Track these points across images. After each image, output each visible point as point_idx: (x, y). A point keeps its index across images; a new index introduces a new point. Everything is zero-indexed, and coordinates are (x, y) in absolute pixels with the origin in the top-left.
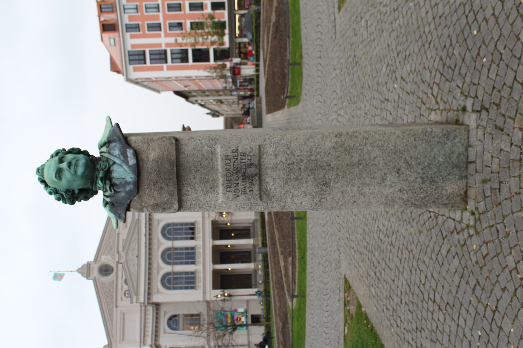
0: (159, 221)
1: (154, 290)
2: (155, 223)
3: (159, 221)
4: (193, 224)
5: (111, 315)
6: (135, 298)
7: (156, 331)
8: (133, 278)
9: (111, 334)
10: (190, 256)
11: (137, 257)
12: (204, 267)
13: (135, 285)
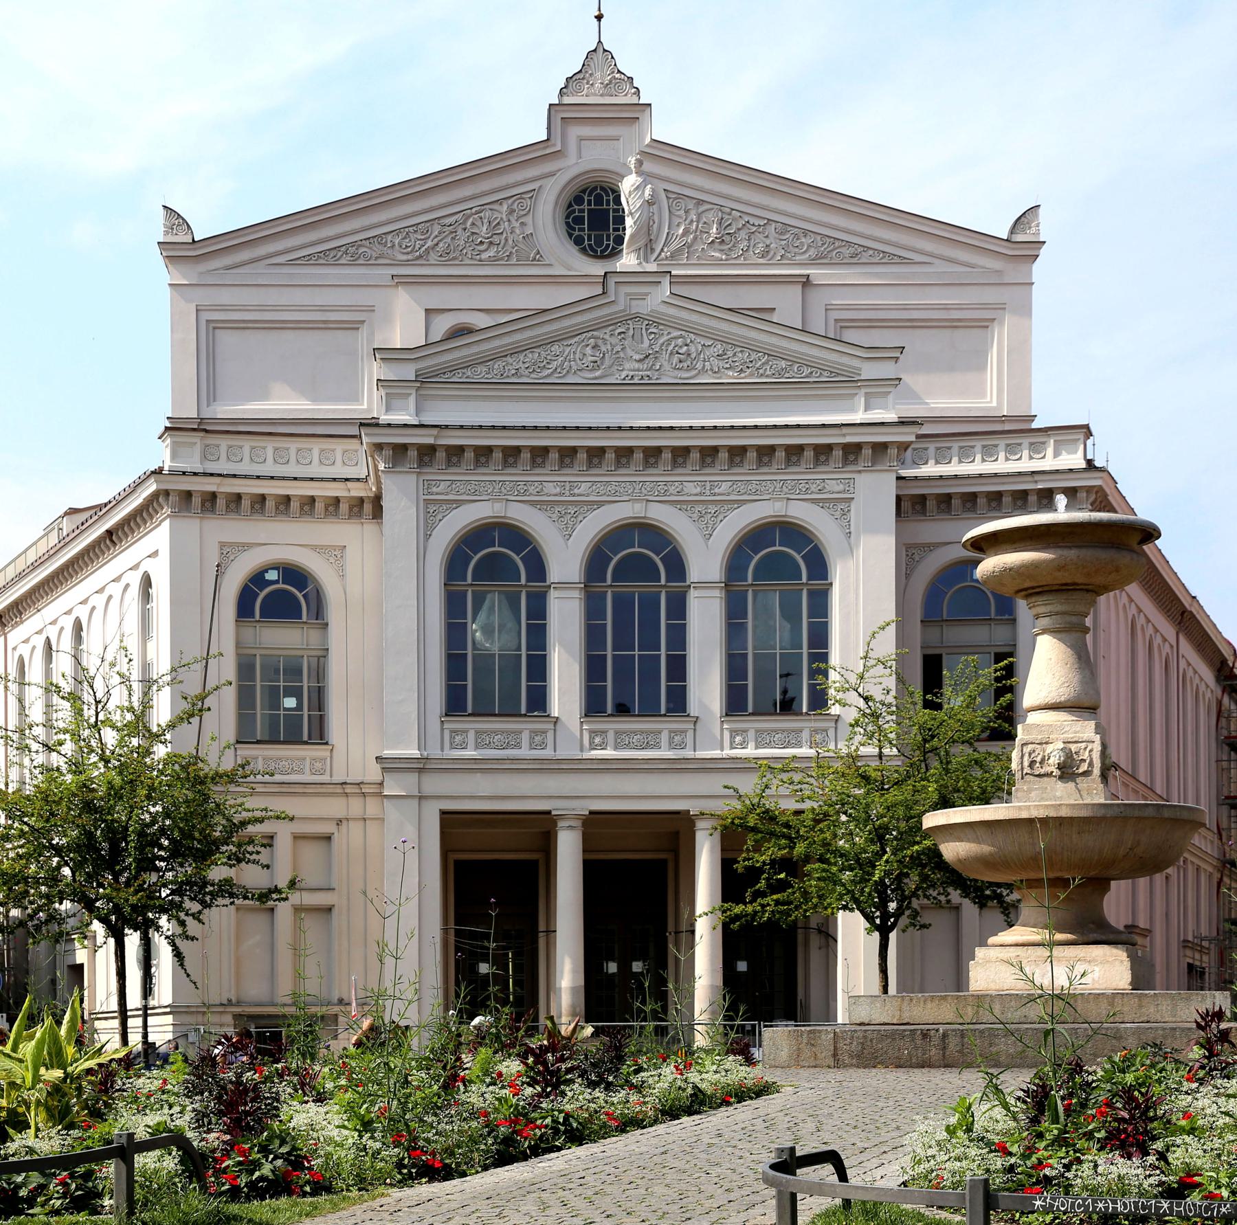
1: (445, 480)
5: (351, 253)
8: (514, 363)
9: (245, 255)
13: (480, 373)
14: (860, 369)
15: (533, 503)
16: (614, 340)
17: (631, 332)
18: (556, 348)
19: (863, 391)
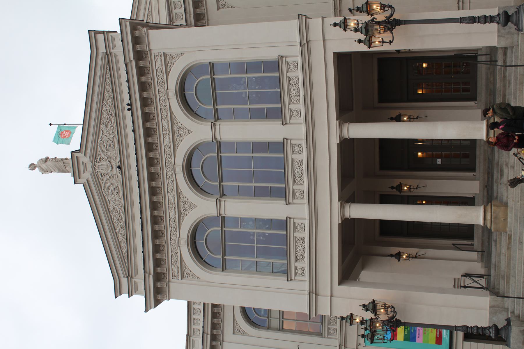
0: (168, 60)
1: (172, 268)
2: (156, 65)
3: (168, 60)
4: (274, 65)
6: (124, 281)
7: (214, 326)
10: (269, 170)
11: (119, 167)
12: (317, 209)
13: (123, 245)
14: (103, 53)
15: (180, 224)
16: (105, 179)
17: (100, 170)
18: (111, 208)
19: (112, 51)
